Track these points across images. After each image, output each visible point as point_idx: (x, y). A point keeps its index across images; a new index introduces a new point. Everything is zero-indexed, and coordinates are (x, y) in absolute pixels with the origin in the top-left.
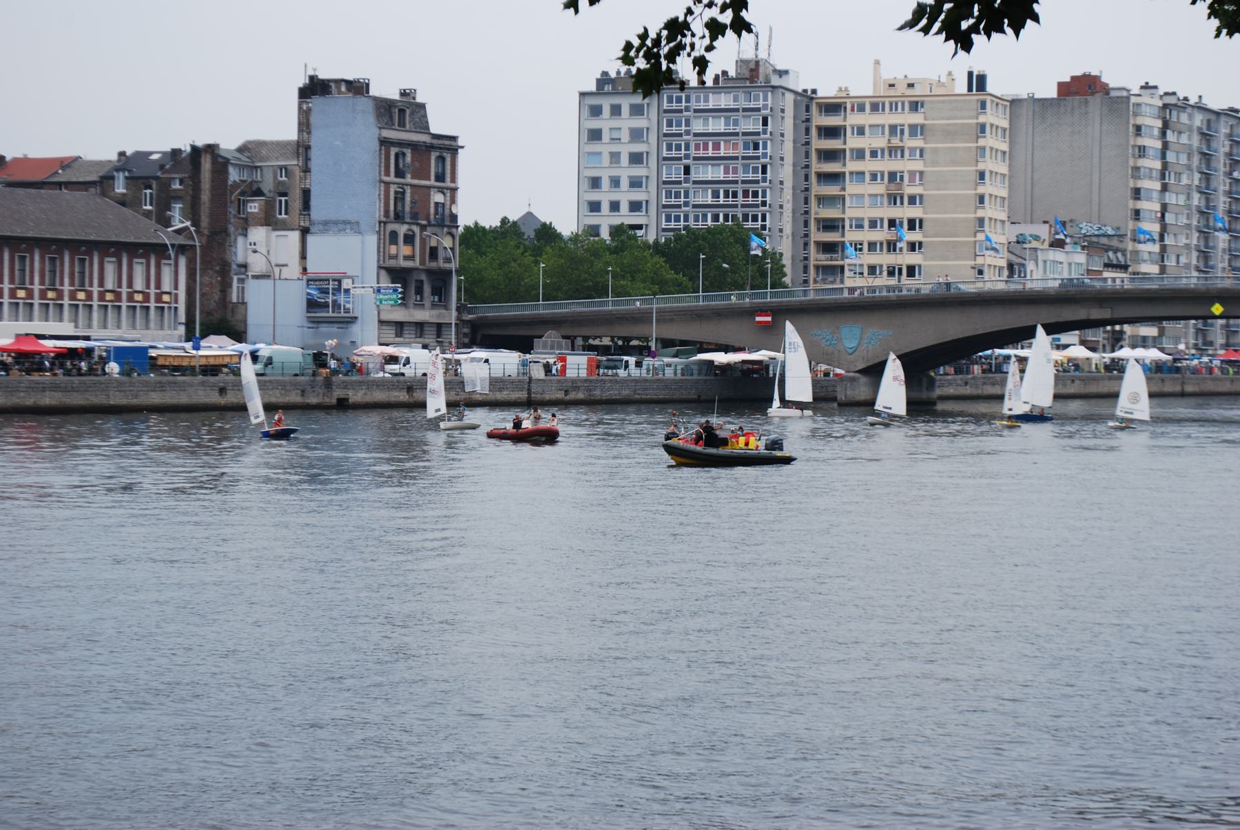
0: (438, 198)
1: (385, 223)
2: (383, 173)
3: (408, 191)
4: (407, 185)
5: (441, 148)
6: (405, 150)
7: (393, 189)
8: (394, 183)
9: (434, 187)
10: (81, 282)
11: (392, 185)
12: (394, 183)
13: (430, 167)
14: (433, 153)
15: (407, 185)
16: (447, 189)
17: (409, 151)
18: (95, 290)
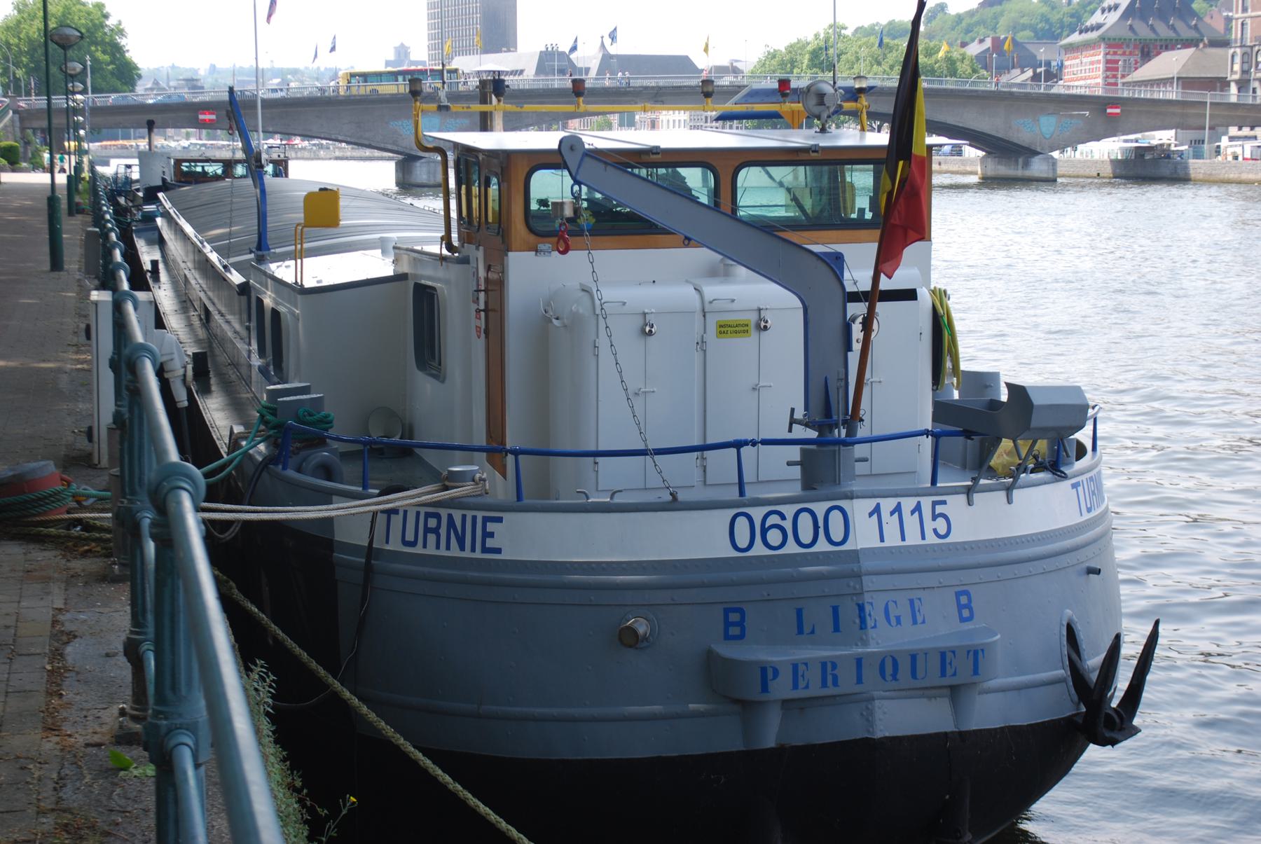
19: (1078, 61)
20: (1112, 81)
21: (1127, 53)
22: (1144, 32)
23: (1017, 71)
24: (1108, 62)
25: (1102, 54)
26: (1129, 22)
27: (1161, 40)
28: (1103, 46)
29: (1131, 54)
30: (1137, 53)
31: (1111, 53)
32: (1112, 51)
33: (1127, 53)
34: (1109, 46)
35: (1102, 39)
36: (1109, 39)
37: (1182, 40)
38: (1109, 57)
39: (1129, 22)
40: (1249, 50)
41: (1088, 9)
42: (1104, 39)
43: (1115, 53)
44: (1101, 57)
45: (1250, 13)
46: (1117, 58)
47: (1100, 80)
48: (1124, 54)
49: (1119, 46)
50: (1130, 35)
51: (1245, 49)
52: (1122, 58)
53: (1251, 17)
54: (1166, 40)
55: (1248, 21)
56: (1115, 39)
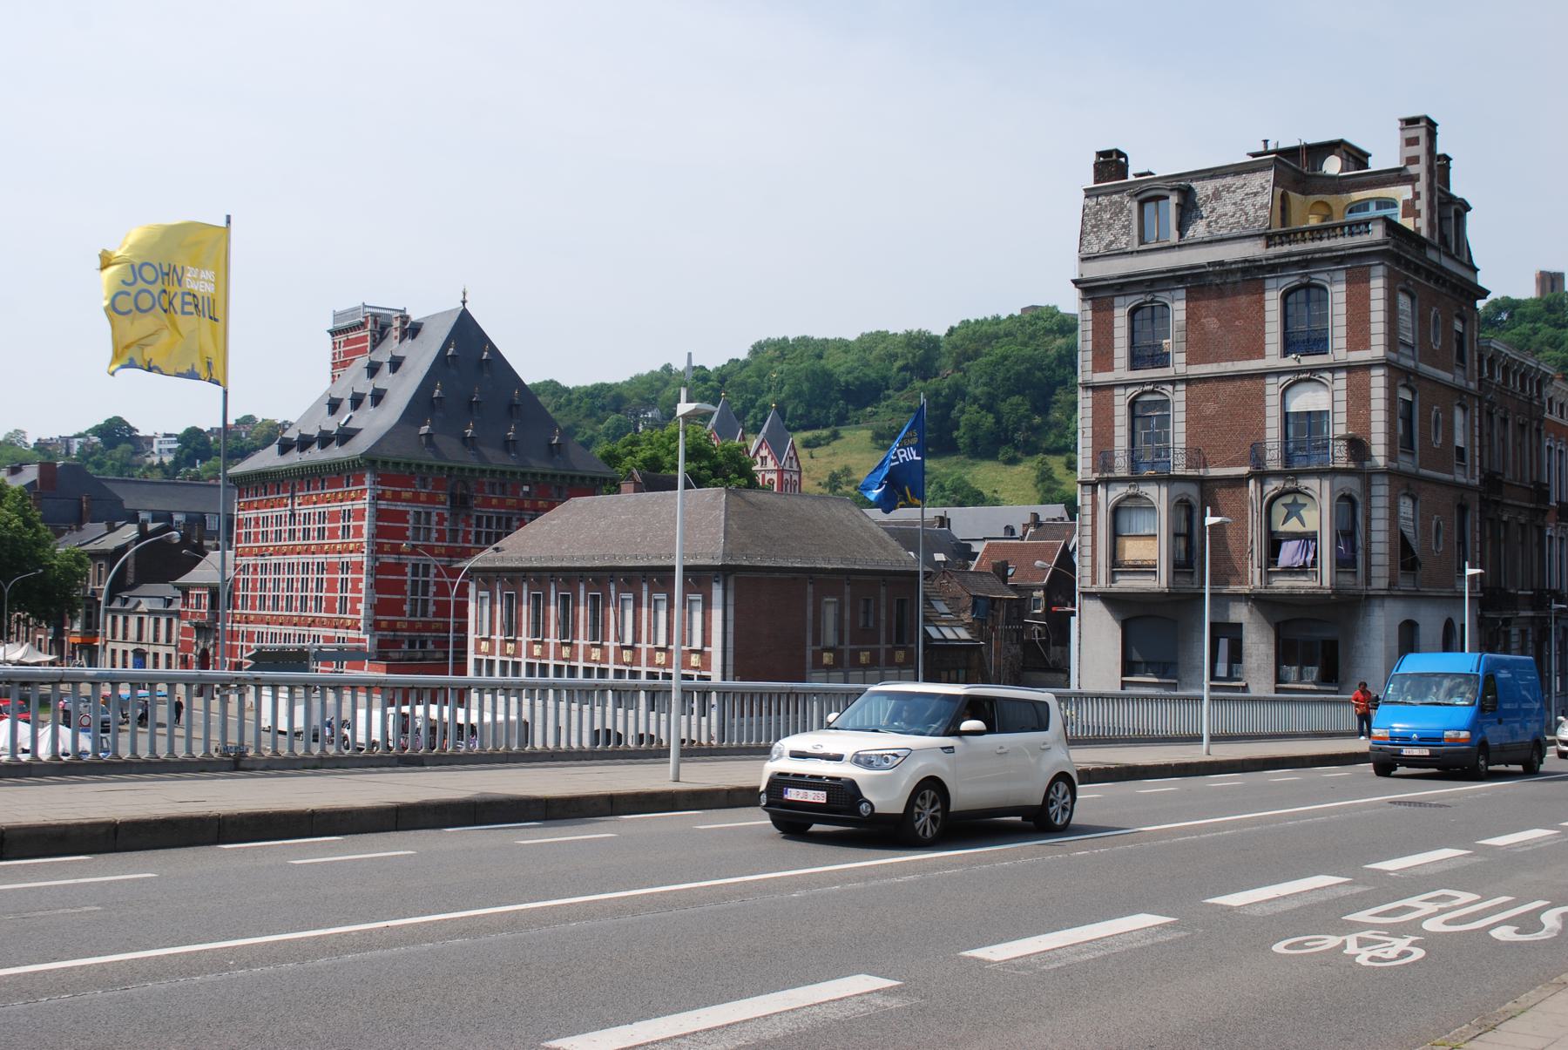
0: (1306, 400)
1: (1094, 485)
2: (1089, 366)
3: (1178, 398)
4: (1173, 382)
5: (1297, 264)
6: (1163, 297)
7: (1121, 400)
8: (1126, 385)
9: (1278, 373)
10: (597, 630)
11: (1117, 391)
12: (1126, 385)
13: (1262, 322)
14: (1269, 284)
15: (1173, 382)
16: (1333, 369)
17: (1182, 294)
18: (611, 644)
19: (284, 512)
20: (390, 559)
21: (423, 498)
22: (454, 454)
23: (102, 527)
24: (380, 515)
25: (367, 496)
26: (425, 429)
27: (493, 472)
28: (368, 479)
29: (431, 499)
30: (442, 498)
31: (388, 495)
32: (389, 489)
33: (423, 498)
34: (383, 479)
35: (370, 461)
36: (385, 463)
37: (534, 475)
38: (383, 505)
39: (425, 429)
40: (1192, 492)
41: (91, 460)
42: (373, 462)
43: (396, 497)
44: (364, 504)
45: (1179, 365)
46: (401, 506)
47: (363, 558)
48: (415, 499)
49: (406, 483)
50: (428, 457)
51: (1180, 489)
52: (411, 509)
53: (1188, 381)
54: (503, 473)
55: (1178, 398)
56: (397, 464)
